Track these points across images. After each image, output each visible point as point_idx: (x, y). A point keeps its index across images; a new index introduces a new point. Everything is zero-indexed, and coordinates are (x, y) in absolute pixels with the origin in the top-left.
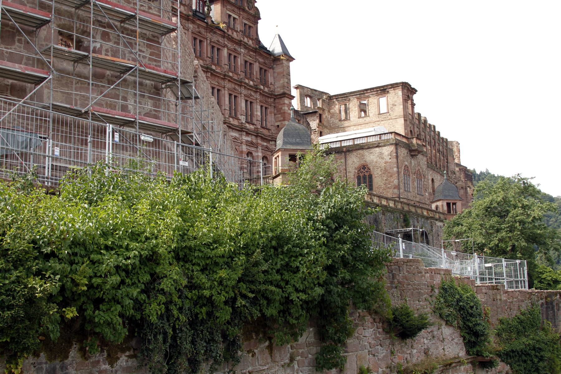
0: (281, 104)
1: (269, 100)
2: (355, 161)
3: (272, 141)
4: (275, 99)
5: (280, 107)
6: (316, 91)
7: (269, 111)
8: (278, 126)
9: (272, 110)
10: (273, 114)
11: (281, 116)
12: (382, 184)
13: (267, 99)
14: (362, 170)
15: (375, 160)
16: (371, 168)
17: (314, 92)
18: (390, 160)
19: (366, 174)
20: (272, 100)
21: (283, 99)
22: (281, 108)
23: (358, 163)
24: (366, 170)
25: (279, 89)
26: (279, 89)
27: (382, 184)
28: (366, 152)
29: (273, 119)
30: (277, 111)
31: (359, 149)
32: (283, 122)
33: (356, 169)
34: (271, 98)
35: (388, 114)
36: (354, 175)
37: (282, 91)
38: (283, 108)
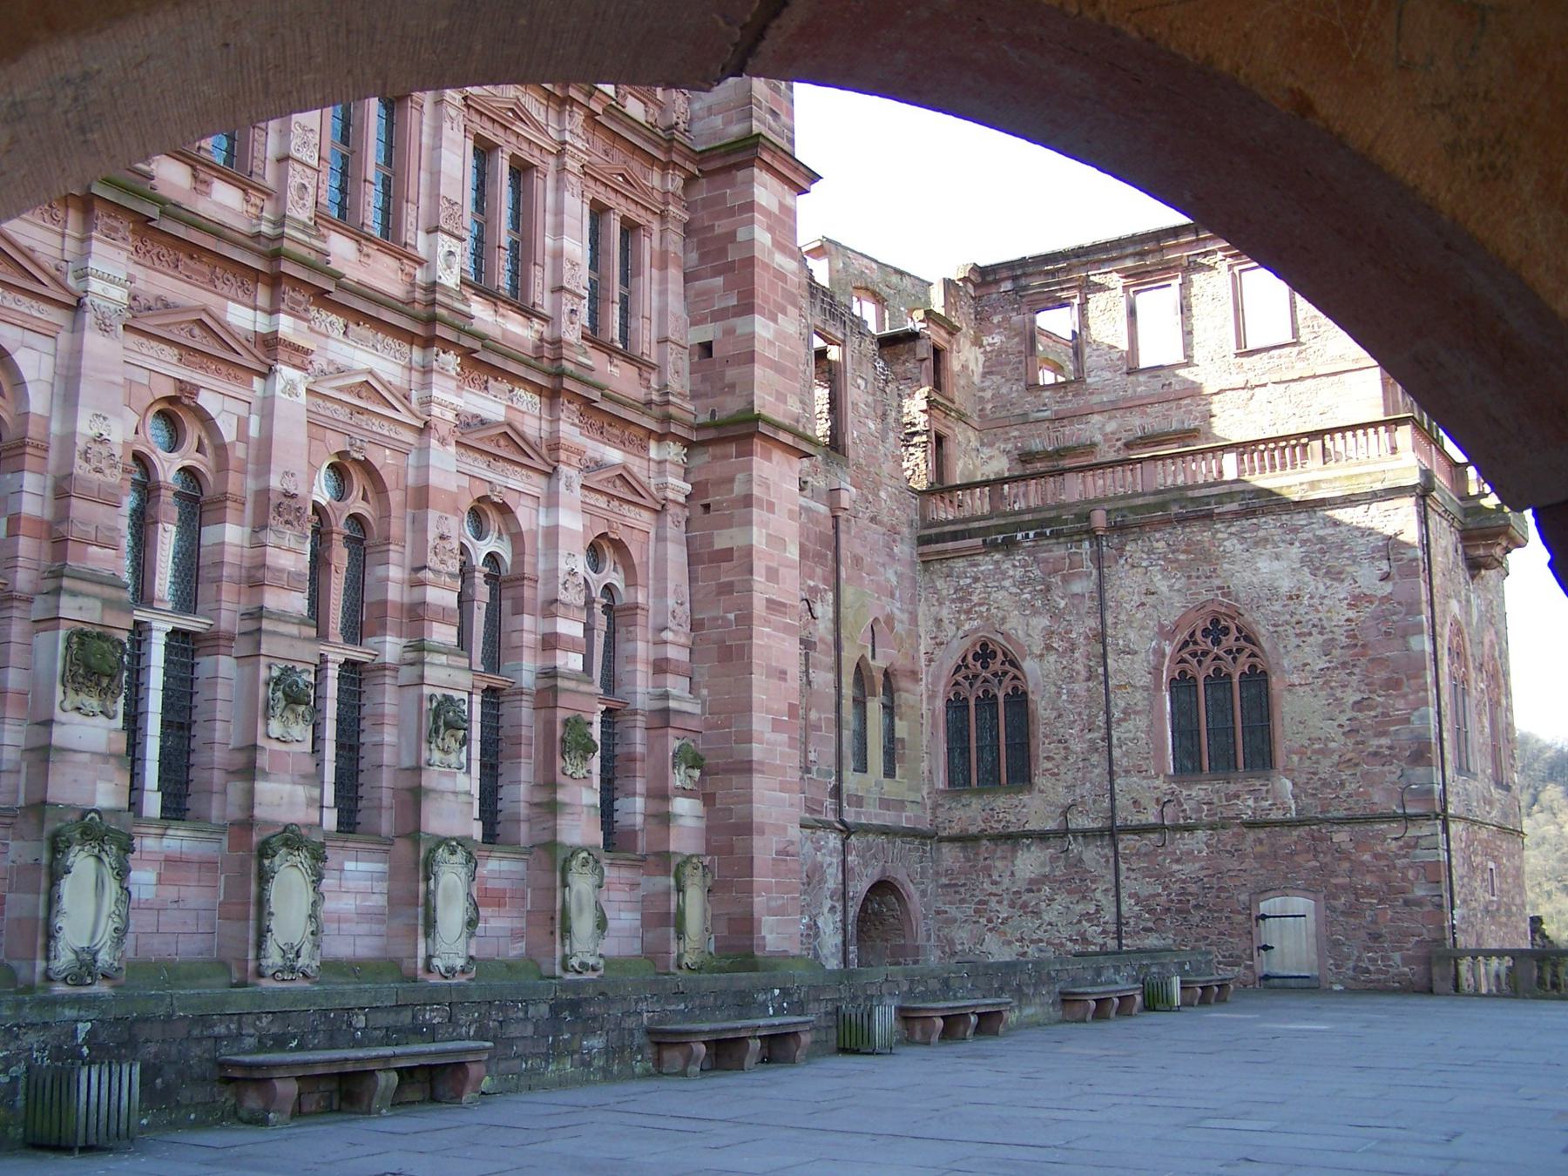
0: (732, 212)
1: (655, 179)
2: (1162, 585)
3: (661, 438)
4: (690, 180)
5: (721, 226)
6: (901, 273)
7: (648, 246)
8: (707, 348)
9: (675, 241)
10: (675, 274)
11: (728, 287)
12: (1330, 729)
13: (636, 166)
14: (1206, 644)
15: (1285, 585)
16: (1263, 631)
17: (895, 279)
18: (1388, 588)
19: (1227, 666)
20: (675, 182)
21: (741, 175)
22: (731, 236)
23: (1178, 602)
24: (1229, 641)
25: (718, 121)
26: (718, 121)
27: (1330, 729)
28: (1227, 539)
29: (676, 304)
30: (703, 257)
31: (1182, 520)
32: (740, 324)
33: (1165, 633)
34: (664, 167)
35: (1295, 350)
36: (1156, 671)
37: (736, 130)
38: (741, 235)
